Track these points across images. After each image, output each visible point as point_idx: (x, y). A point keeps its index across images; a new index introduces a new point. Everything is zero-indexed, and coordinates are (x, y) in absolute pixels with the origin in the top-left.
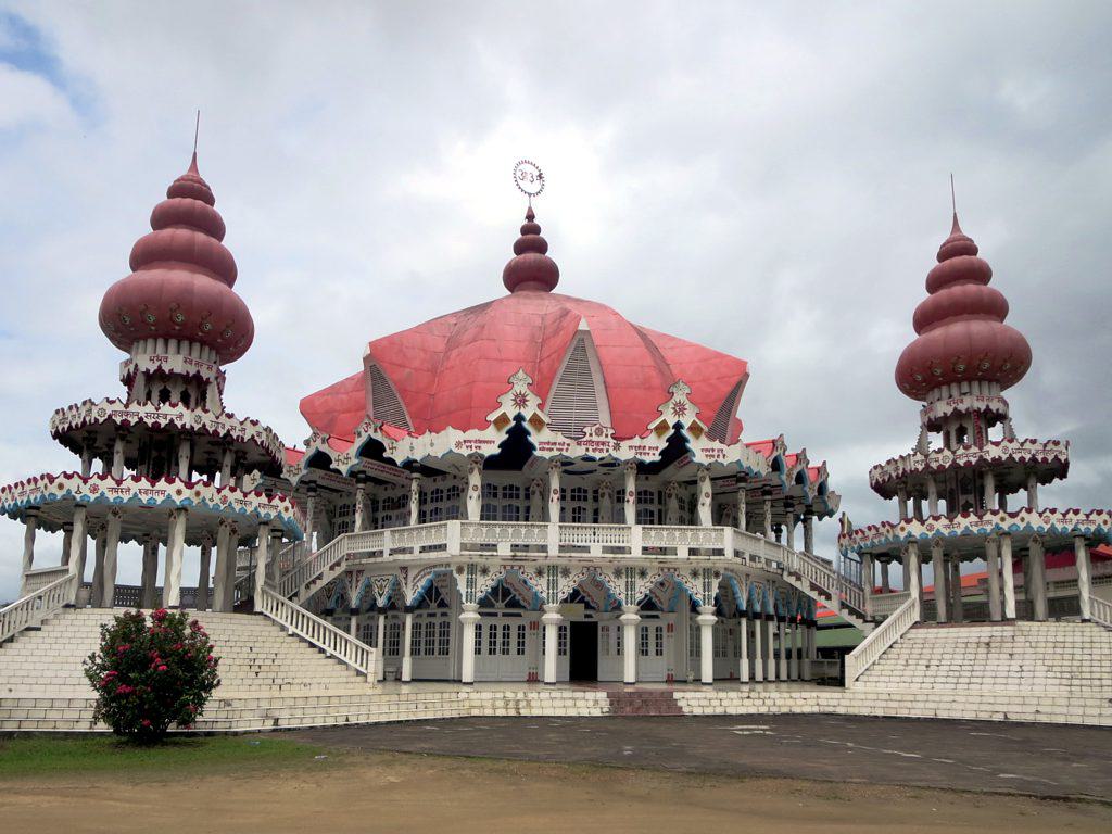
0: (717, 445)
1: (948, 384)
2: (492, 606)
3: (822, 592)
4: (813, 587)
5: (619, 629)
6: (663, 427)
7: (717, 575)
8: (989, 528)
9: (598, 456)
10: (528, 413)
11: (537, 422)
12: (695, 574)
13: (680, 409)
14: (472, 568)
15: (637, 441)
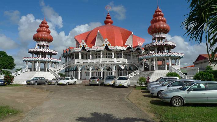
0: (113, 47)
1: (155, 33)
2: (109, 69)
3: (138, 66)
4: (137, 66)
5: (89, 73)
6: (104, 45)
7: (115, 65)
8: (164, 55)
9: (95, 50)
10: (84, 45)
11: (86, 46)
12: (111, 65)
13: (106, 42)
14: (79, 65)
15: (100, 47)
